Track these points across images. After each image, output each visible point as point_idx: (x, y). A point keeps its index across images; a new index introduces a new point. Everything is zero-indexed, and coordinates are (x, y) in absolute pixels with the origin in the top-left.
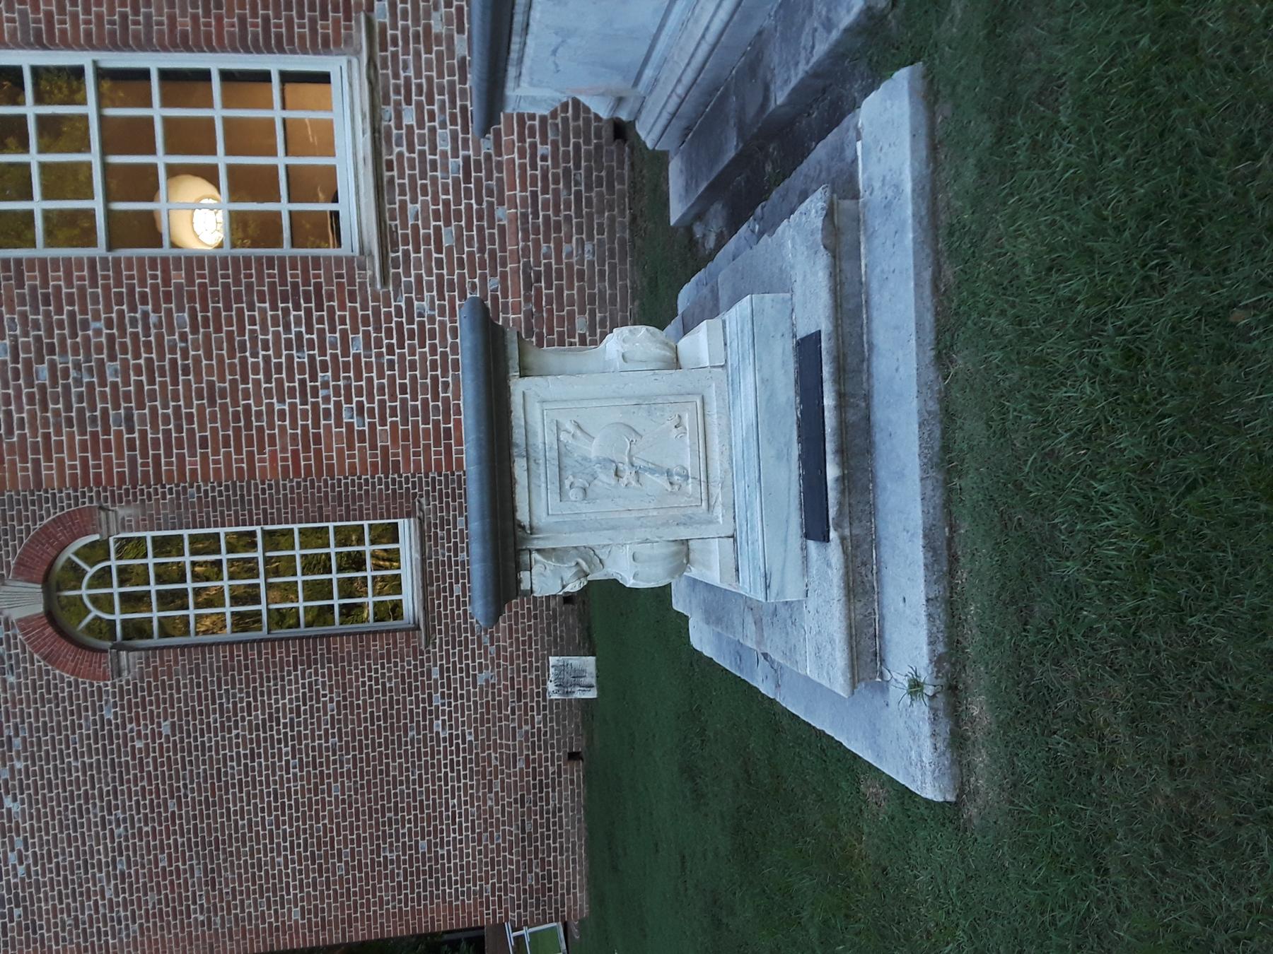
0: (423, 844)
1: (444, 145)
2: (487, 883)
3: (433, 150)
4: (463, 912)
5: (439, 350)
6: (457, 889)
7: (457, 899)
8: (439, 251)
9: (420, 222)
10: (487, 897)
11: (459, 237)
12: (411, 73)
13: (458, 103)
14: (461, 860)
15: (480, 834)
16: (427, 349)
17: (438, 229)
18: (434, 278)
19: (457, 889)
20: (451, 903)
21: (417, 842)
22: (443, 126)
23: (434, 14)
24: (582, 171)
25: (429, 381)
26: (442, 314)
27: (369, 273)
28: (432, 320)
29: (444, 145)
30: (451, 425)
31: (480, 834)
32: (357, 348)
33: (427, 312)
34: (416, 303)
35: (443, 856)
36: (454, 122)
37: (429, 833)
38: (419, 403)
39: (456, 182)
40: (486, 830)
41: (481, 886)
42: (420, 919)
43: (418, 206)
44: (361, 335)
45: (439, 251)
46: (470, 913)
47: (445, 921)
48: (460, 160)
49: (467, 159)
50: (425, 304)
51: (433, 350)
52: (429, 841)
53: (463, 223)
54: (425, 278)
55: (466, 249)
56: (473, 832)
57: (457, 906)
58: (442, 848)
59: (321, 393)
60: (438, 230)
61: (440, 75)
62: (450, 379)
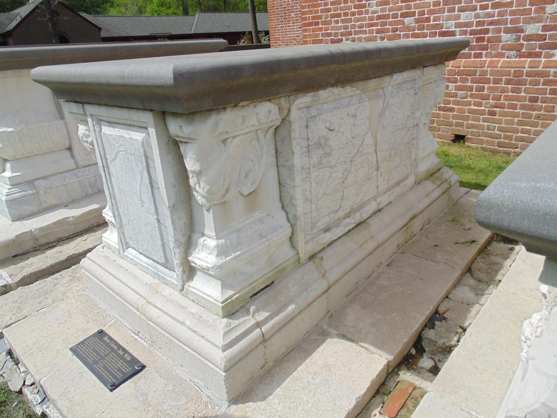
0: (293, 15)
1: (465, 17)
2: (282, 43)
3: (462, 10)
4: (274, 33)
5: (353, 17)
6: (280, 30)
7: (278, 30)
8: (403, 15)
10: (277, 43)
11: (408, 28)
14: (289, 32)
15: (295, 40)
16: (353, 10)
17: (413, 14)
18: (387, 13)
19: (280, 30)
20: (276, 27)
21: (294, 12)
22: (477, 16)
24: (437, 111)
25: (339, 12)
26: (371, 19)
28: (367, 12)
29: (465, 17)
30: (320, 26)
31: (295, 40)
33: (371, 10)
35: (289, 23)
36: (479, 24)
37: (296, 17)
38: (329, 6)
39: (441, 26)
40: (297, 42)
41: (280, 40)
42: (272, 15)
45: (403, 15)
46: (273, 35)
47: (271, 25)
48: (453, 29)
50: (375, 8)
51: (353, 14)
52: (294, 17)
53: (416, 31)
54: (388, 7)
55: (402, 33)
56: (297, 36)
57: (275, 30)
58: (293, 23)
60: (413, 14)
61: (513, 13)
62: (339, 24)
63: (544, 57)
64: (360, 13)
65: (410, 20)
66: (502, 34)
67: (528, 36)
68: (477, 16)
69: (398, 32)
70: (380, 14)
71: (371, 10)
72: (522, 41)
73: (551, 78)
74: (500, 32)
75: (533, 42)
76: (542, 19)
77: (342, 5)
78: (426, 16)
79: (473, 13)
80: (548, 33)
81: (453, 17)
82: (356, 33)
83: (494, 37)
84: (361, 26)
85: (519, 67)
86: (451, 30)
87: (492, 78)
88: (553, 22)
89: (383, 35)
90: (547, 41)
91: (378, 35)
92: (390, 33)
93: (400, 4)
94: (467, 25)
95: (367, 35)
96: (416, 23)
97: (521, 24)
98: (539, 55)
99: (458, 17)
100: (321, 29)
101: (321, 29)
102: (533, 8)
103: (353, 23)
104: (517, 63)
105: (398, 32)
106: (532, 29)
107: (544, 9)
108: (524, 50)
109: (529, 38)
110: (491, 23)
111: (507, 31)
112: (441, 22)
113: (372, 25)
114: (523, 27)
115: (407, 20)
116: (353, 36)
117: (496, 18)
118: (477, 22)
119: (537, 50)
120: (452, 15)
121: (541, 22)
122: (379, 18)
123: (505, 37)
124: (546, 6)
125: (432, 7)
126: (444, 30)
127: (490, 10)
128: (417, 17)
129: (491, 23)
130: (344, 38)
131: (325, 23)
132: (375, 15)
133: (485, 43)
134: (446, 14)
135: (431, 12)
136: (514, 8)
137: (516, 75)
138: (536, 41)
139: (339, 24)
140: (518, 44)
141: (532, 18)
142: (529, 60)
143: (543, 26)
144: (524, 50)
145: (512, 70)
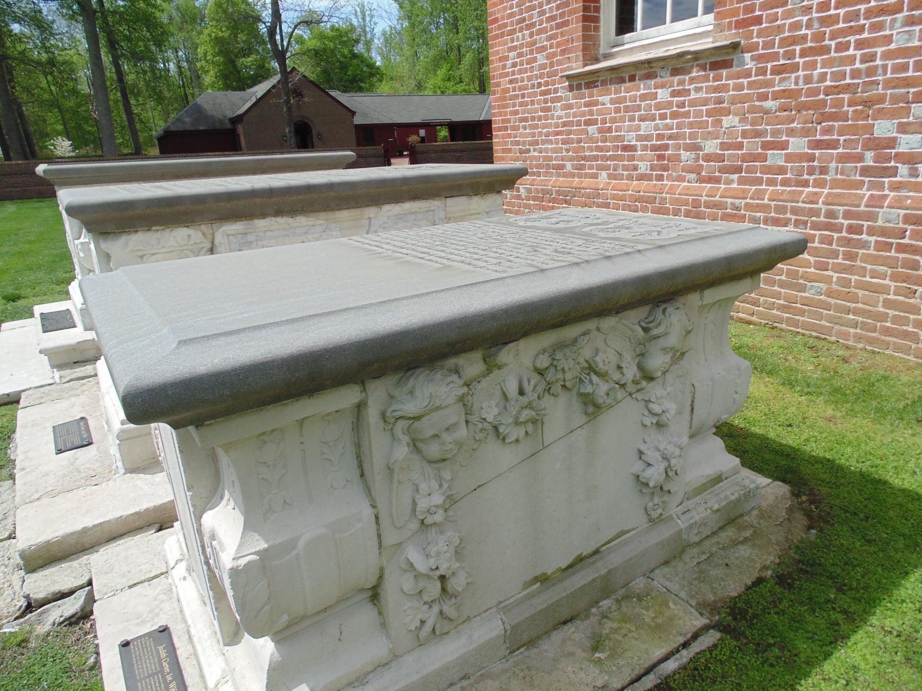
1: (646, 128)
9: (600, 107)
12: (693, 95)
13: (670, 142)
16: (540, 114)
18: (571, 119)
22: (656, 128)
23: (737, 119)
26: (557, 125)
27: (574, 65)
32: (541, 59)
34: (559, 104)
38: (517, 108)
43: (609, 105)
44: (545, 61)
49: (633, 148)
50: (560, 113)
51: (540, 119)
53: (599, 144)
55: (586, 145)
59: (520, 35)
62: (527, 131)
63: (724, 184)
64: (546, 117)
65: (593, 129)
66: (682, 152)
67: (707, 155)
68: (656, 128)
69: (582, 144)
70: (565, 120)
71: (556, 114)
72: (701, 162)
73: (728, 210)
74: (680, 148)
75: (712, 163)
76: (719, 134)
77: (529, 107)
78: (608, 125)
79: (653, 123)
80: (726, 152)
81: (634, 127)
82: (544, 142)
83: (674, 154)
84: (547, 135)
85: (696, 195)
86: (632, 143)
87: (671, 207)
88: (730, 139)
89: (567, 146)
90: (725, 163)
91: (563, 146)
92: (575, 145)
93: (583, 109)
94: (647, 138)
95: (553, 146)
96: (599, 133)
97: (699, 140)
98: (718, 181)
99: (638, 128)
100: (509, 136)
101: (509, 136)
102: (710, 119)
103: (540, 130)
104: (695, 190)
105: (582, 144)
106: (711, 146)
107: (720, 121)
108: (703, 173)
109: (708, 158)
110: (670, 137)
111: (688, 148)
112: (622, 133)
113: (557, 134)
114: (702, 144)
115: (592, 129)
116: (540, 146)
117: (675, 131)
118: (657, 134)
119: (717, 174)
120: (633, 125)
121: (718, 138)
122: (565, 124)
123: (685, 155)
124: (722, 118)
125: (613, 115)
126: (625, 143)
127: (668, 121)
128: (599, 126)
129: (670, 137)
130: (531, 148)
131: (515, 128)
132: (560, 121)
133: (666, 162)
134: (627, 123)
135: (613, 120)
136: (691, 119)
137: (694, 205)
138: (715, 162)
139: (527, 131)
140: (698, 165)
141: (709, 133)
142: (709, 185)
143: (721, 143)
144: (703, 173)
145: (691, 198)
